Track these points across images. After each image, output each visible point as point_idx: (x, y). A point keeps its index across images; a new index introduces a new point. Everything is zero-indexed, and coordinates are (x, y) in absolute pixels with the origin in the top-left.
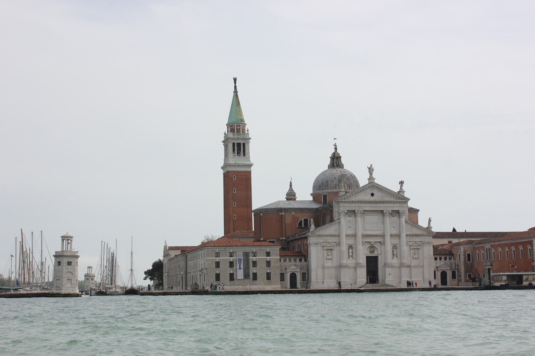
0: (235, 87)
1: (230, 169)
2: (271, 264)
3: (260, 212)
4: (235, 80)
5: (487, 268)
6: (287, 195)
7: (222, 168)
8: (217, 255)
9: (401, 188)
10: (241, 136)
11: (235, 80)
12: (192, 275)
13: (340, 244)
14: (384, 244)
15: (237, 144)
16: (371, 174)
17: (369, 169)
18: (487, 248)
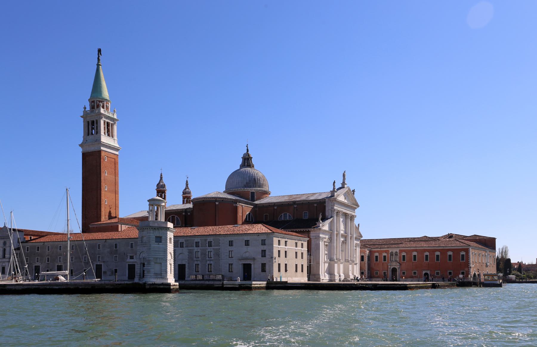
3: (216, 201)
17: (344, 175)
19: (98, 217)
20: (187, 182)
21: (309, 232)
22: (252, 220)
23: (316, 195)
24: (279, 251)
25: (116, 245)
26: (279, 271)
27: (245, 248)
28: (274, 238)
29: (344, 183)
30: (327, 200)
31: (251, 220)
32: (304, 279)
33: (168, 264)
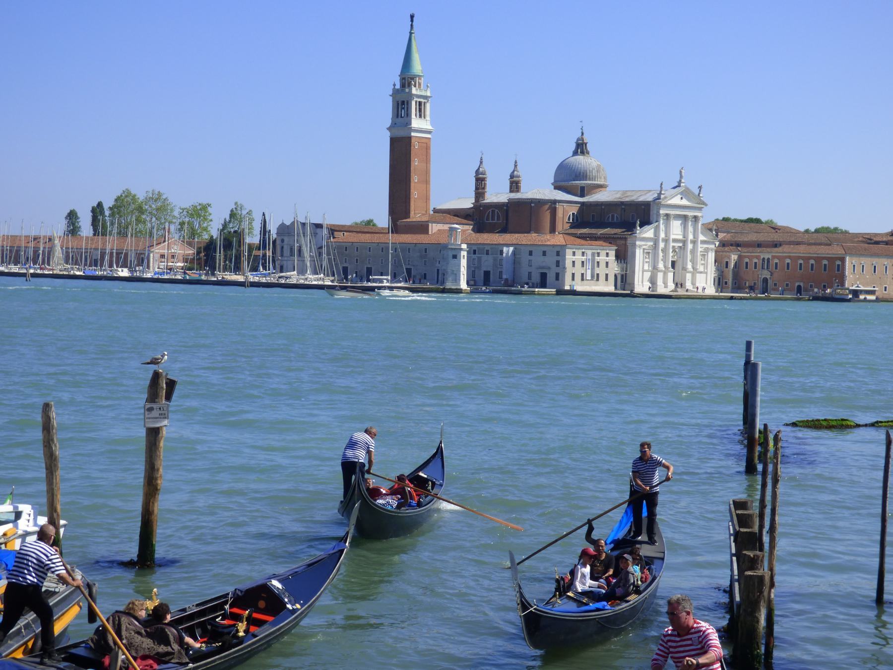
0: (412, 25)
1: (413, 134)
2: (610, 265)
4: (412, 17)
5: (763, 277)
6: (477, 172)
7: (389, 129)
8: (574, 254)
9: (699, 194)
10: (423, 93)
11: (412, 17)
12: (484, 269)
13: (655, 247)
14: (684, 249)
15: (419, 102)
16: (681, 177)
17: (681, 172)
18: (764, 259)
19: (407, 214)
20: (516, 162)
21: (626, 239)
22: (577, 220)
23: (651, 193)
24: (574, 262)
25: (426, 249)
26: (573, 279)
27: (542, 258)
28: (567, 250)
29: (680, 182)
30: (651, 203)
31: (575, 221)
32: (611, 289)
33: (461, 274)
